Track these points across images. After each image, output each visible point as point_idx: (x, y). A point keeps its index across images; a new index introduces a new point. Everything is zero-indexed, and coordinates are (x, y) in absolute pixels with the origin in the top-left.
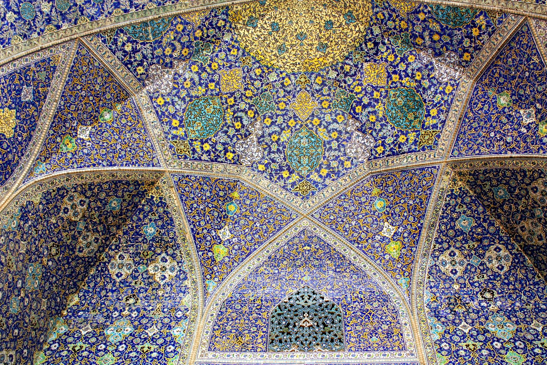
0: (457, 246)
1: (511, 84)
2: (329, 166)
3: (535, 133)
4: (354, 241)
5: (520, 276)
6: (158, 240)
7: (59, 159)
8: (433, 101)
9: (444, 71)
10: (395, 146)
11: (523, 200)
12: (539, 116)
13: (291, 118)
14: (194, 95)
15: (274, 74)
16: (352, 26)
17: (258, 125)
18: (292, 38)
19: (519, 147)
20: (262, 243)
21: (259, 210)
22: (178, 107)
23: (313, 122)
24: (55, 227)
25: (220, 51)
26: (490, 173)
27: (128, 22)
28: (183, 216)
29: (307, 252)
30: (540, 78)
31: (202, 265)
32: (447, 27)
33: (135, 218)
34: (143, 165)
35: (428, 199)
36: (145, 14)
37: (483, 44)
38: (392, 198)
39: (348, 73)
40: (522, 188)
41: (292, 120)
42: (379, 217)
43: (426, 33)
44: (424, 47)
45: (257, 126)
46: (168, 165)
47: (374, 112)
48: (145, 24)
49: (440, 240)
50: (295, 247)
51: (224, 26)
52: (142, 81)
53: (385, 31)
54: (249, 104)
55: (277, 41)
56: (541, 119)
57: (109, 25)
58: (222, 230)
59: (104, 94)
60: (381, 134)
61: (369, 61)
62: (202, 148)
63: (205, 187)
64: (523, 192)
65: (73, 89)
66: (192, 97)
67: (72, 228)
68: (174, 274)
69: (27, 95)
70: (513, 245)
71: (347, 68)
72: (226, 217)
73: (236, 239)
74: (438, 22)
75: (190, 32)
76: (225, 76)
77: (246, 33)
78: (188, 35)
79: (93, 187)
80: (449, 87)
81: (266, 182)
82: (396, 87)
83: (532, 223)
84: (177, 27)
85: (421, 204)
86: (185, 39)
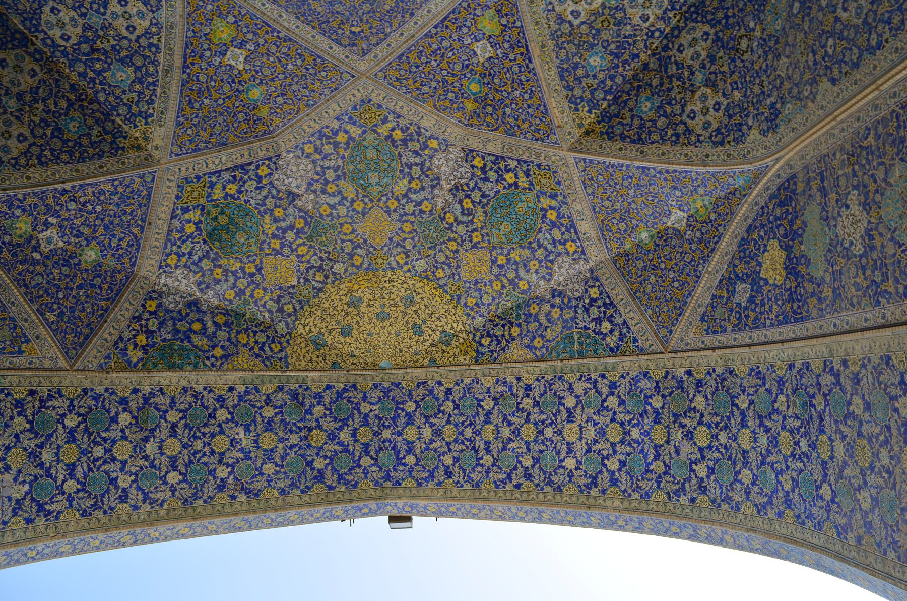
0: (126, 42)
1: (83, 278)
2: (336, 145)
3: (36, 219)
4: (285, 41)
7: (716, 188)
8: (193, 243)
9: (183, 283)
10: (241, 179)
11: (37, 120)
12: (34, 242)
13: (394, 211)
14: (526, 250)
15: (420, 269)
16: (315, 331)
17: (440, 202)
18: (396, 314)
19: (54, 197)
20: (426, 35)
21: (434, 84)
22: (548, 236)
23: (362, 205)
24: (736, 83)
25: (489, 304)
26: (94, 155)
27: (602, 360)
28: (544, 84)
29: (355, 23)
30: (41, 293)
32: (182, 341)
33: (619, 80)
34: (599, 163)
35: (181, 110)
36: (579, 369)
37: (129, 326)
38: (237, 104)
39: (318, 271)
40: (42, 137)
41: (392, 207)
42: (253, 76)
43: (211, 330)
44: (214, 311)
45: (441, 200)
46: (564, 159)
47: (276, 220)
48: (581, 355)
49: (153, 49)
50: (374, 31)
51: (482, 337)
52: (593, 278)
53: (269, 327)
54: (452, 232)
55: (416, 312)
57: (626, 361)
58: (487, 56)
60: (264, 192)
61: (289, 288)
62: (516, 176)
63: (512, 120)
64: (39, 131)
65: (683, 284)
66: (528, 248)
67: (713, 77)
71: (319, 277)
72: (483, 75)
73: (466, 43)
74: (195, 347)
75: (526, 335)
76: (484, 272)
77: (455, 325)
78: (528, 331)
79: (674, 138)
81: (425, 123)
82: (248, 257)
83: (19, 84)
84: (541, 345)
85: (190, 100)
86: (533, 326)
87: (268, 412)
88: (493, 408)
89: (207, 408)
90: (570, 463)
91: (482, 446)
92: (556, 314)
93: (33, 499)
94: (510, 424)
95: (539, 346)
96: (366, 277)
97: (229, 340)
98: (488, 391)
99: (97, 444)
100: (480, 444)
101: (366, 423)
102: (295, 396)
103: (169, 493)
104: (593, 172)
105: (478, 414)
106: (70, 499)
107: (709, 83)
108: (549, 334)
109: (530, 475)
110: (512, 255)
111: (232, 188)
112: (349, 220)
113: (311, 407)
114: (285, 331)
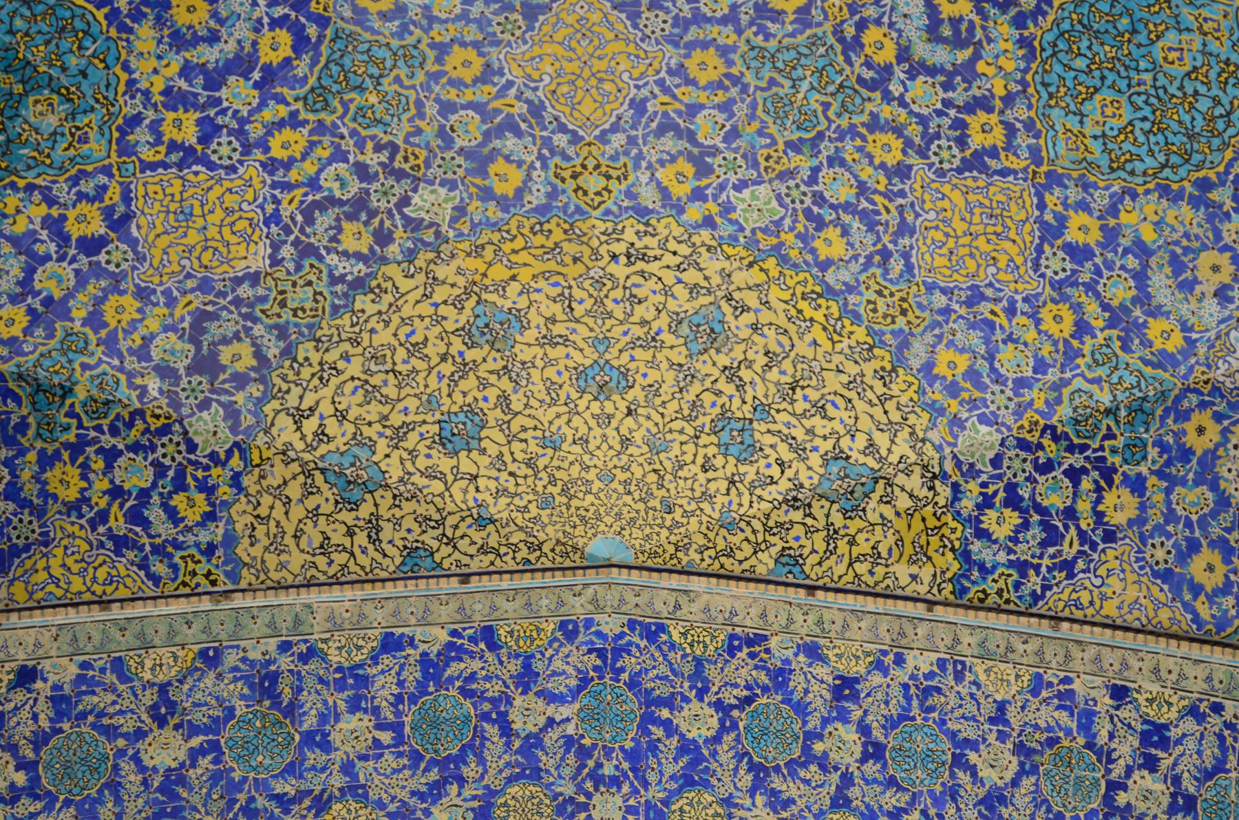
14: (1186, 210)
15: (752, 221)
18: (654, 375)
25: (1021, 383)
39: (352, 217)
47: (180, 40)
51: (987, 502)
53: (165, 430)
54: (887, 97)
55: (731, 373)
61: (238, 281)
66: (1195, 202)
71: (356, 238)
76: (1007, 263)
77: (882, 440)
78: (1170, 516)
82: (75, 181)
87: (166, 751)
88: (1015, 783)
95: (1211, 581)
96: (539, 240)
98: (1000, 715)
102: (264, 683)
105: (953, 793)
110: (1124, 218)
112: (472, 33)
113: (323, 719)
114: (226, 438)
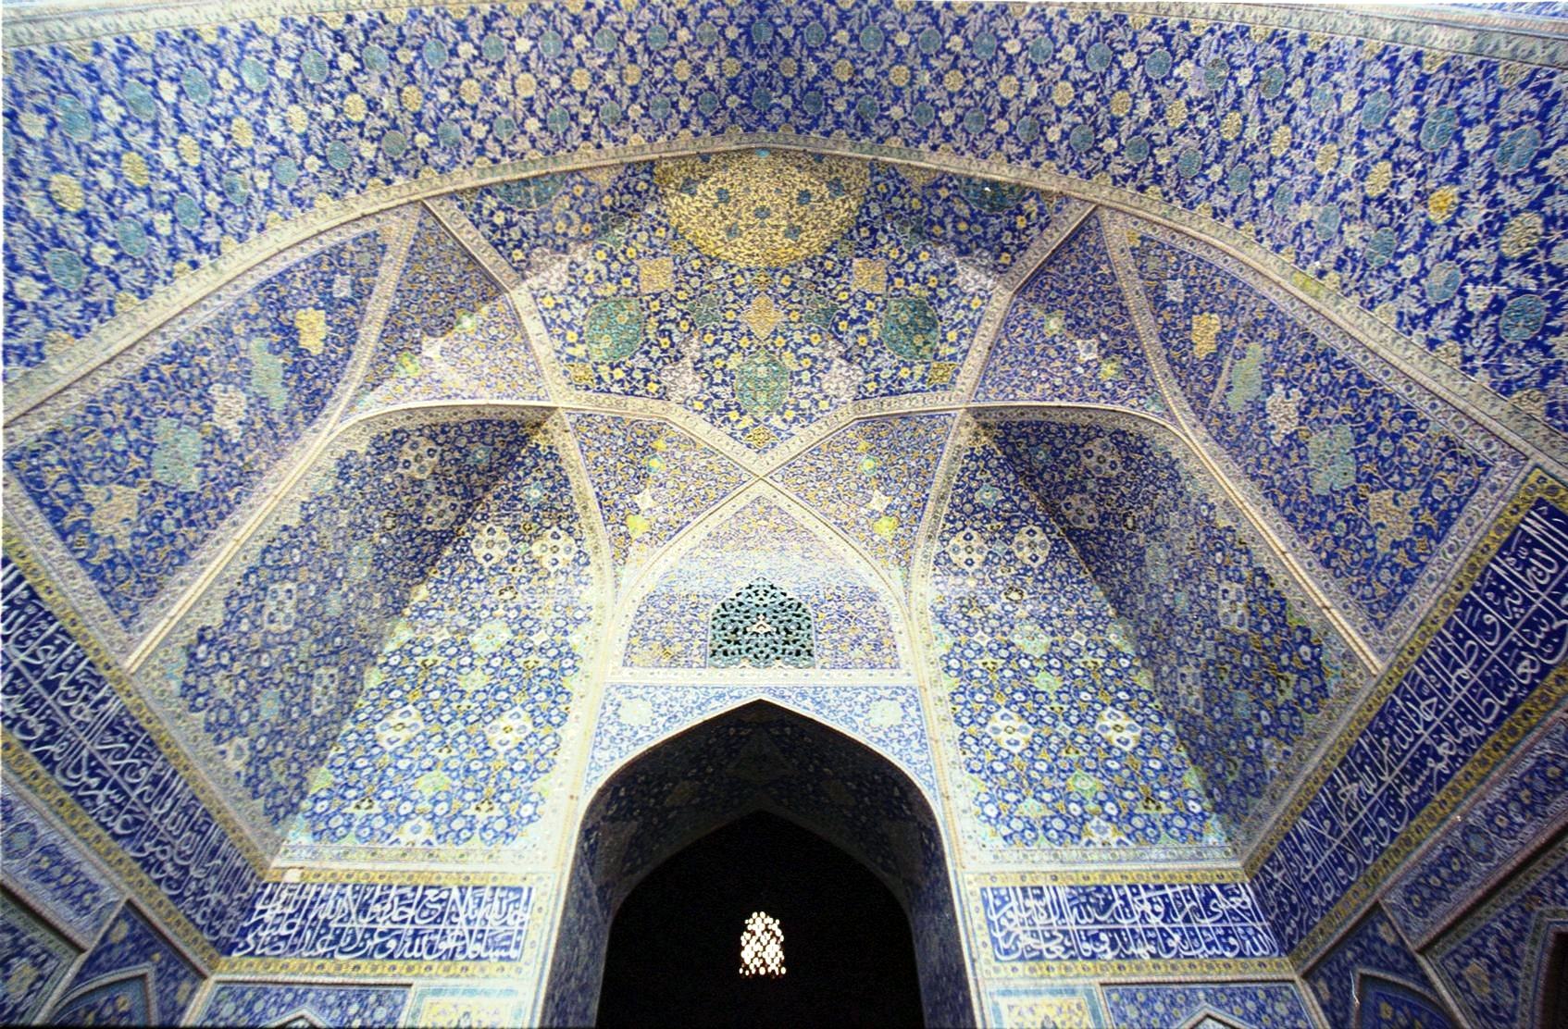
2: (797, 408)
5: (1060, 571)
6: (546, 508)
9: (970, 277)
16: (838, 202)
17: (695, 343)
27: (498, 179)
31: (612, 544)
33: (511, 476)
35: (937, 460)
43: (948, 220)
44: (942, 241)
47: (866, 332)
48: (525, 182)
52: (521, 270)
55: (725, 218)
56: (1106, 356)
57: (469, 183)
59: (462, 289)
60: (874, 364)
63: (617, 432)
64: (1072, 457)
68: (570, 557)
69: (342, 288)
70: (1052, 527)
80: (977, 300)
86: (587, 209)
87: (896, 112)
89: (963, 130)
90: (523, 45)
91: (639, 57)
92: (561, 226)
93: (1174, 54)
94: (606, 88)
97: (931, 205)
99: (1089, 109)
100: (643, 59)
101: (787, 81)
103: (1021, 27)
104: (531, 388)
105: (648, 97)
106: (1134, 43)
107: (421, 483)
108: (566, 202)
109: (574, 23)
111: (904, 373)
